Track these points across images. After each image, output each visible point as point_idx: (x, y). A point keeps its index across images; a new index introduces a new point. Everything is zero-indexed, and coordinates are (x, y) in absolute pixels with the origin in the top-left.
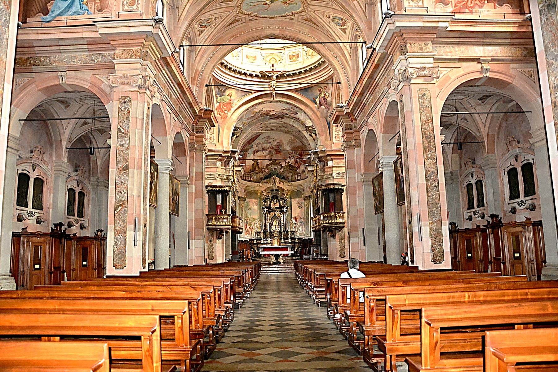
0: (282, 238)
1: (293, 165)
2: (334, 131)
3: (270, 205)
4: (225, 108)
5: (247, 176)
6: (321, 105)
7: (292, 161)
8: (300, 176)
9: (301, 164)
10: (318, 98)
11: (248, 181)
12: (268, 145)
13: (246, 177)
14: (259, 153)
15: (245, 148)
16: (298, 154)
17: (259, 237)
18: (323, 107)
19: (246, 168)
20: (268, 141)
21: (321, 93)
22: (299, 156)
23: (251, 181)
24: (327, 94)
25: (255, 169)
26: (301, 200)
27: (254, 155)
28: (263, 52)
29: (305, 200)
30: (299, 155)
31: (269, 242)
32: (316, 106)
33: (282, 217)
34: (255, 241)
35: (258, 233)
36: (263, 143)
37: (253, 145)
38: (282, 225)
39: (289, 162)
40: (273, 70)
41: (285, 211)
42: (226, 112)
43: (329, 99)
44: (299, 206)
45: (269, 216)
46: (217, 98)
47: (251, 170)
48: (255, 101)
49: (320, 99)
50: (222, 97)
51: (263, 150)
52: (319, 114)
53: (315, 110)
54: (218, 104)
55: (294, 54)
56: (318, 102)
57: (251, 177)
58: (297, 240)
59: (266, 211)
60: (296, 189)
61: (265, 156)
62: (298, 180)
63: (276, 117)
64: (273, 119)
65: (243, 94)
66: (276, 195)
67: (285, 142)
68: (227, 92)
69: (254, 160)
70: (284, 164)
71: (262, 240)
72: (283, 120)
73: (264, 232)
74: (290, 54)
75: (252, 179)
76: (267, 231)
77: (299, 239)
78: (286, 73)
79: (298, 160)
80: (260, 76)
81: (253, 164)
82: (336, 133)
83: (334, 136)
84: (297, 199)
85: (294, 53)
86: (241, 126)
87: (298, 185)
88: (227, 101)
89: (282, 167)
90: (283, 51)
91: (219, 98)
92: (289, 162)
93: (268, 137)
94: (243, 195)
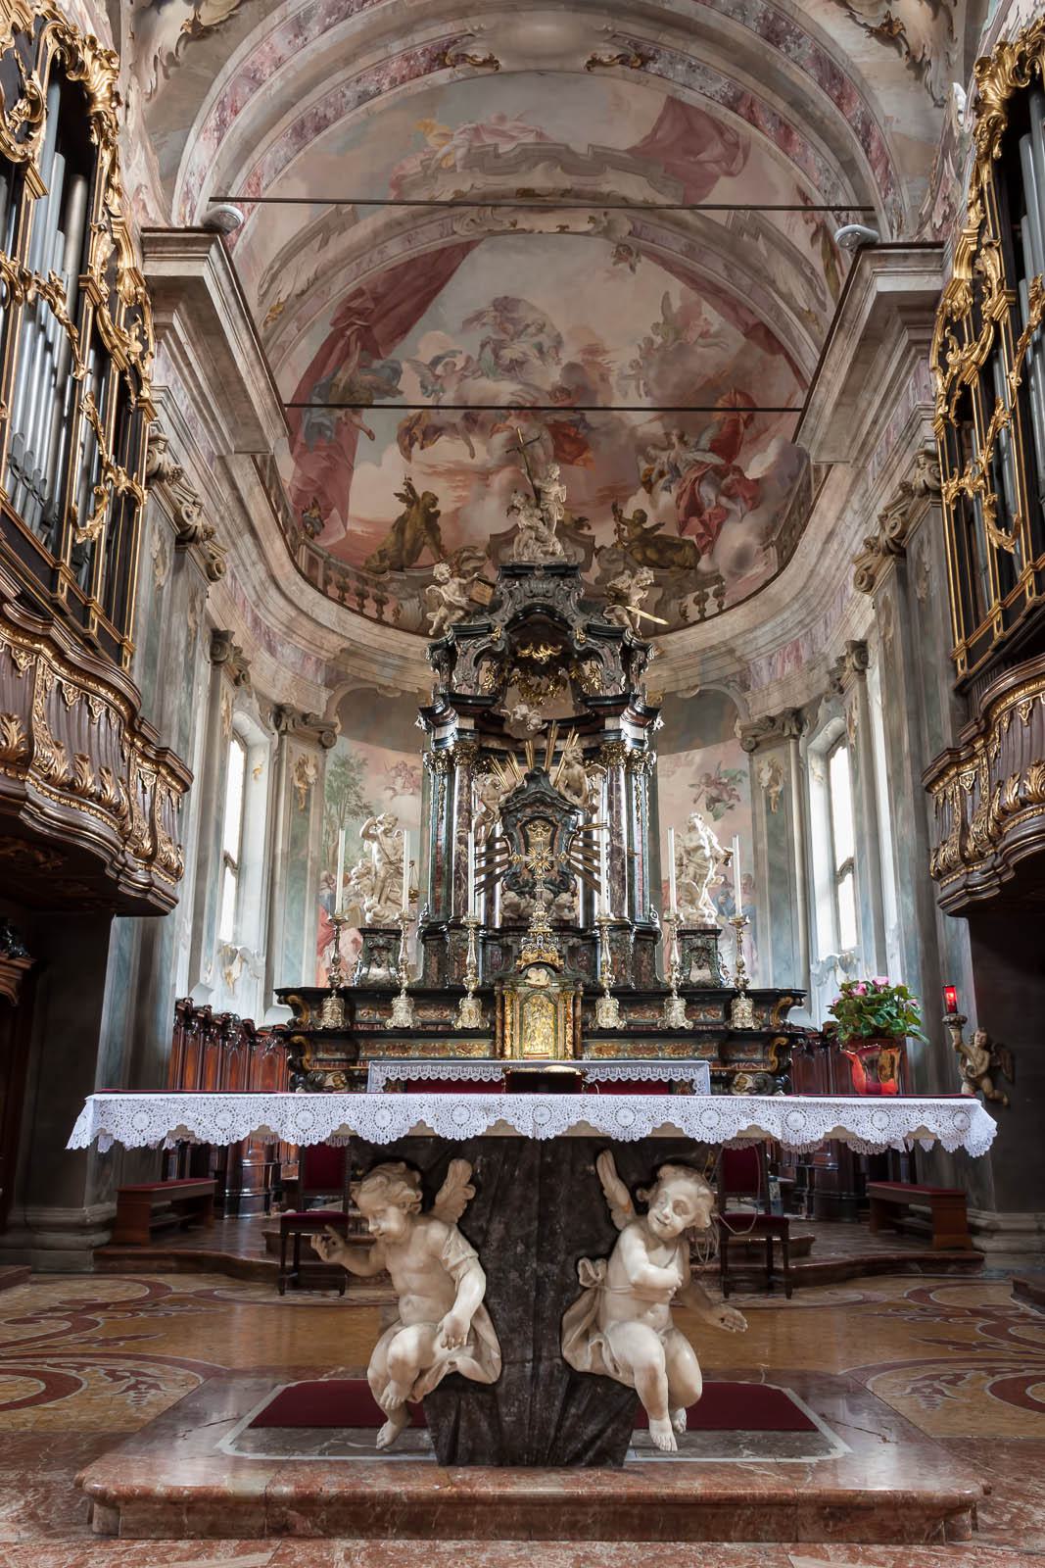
0: (606, 979)
1: (670, 531)
3: (497, 695)
5: (353, 584)
7: (659, 507)
8: (718, 594)
9: (728, 512)
11: (361, 614)
12: (505, 390)
13: (343, 588)
14: (448, 450)
15: (343, 377)
16: (705, 442)
17: (378, 973)
19: (350, 534)
20: (508, 354)
22: (714, 459)
23: (379, 621)
25: (414, 554)
26: (728, 755)
27: (407, 452)
29: (754, 748)
30: (712, 450)
31: (469, 1013)
33: (601, 801)
34: (331, 1005)
35: (379, 939)
36: (472, 369)
37: (397, 373)
38: (604, 864)
39: (642, 517)
41: (629, 746)
44: (712, 802)
45: (482, 784)
47: (382, 555)
51: (474, 417)
57: (381, 602)
58: (744, 1008)
59: (450, 743)
60: (688, 683)
61: (484, 475)
62: (704, 619)
66: (550, 611)
67: (621, 357)
69: (409, 496)
70: (604, 534)
71: (401, 1003)
73: (431, 934)
75: (388, 616)
76: (458, 926)
77: (765, 999)
79: (707, 493)
81: (400, 525)
84: (697, 755)
87: (707, 654)
89: (592, 550)
92: (642, 517)
93: (505, 306)
94: (318, 702)
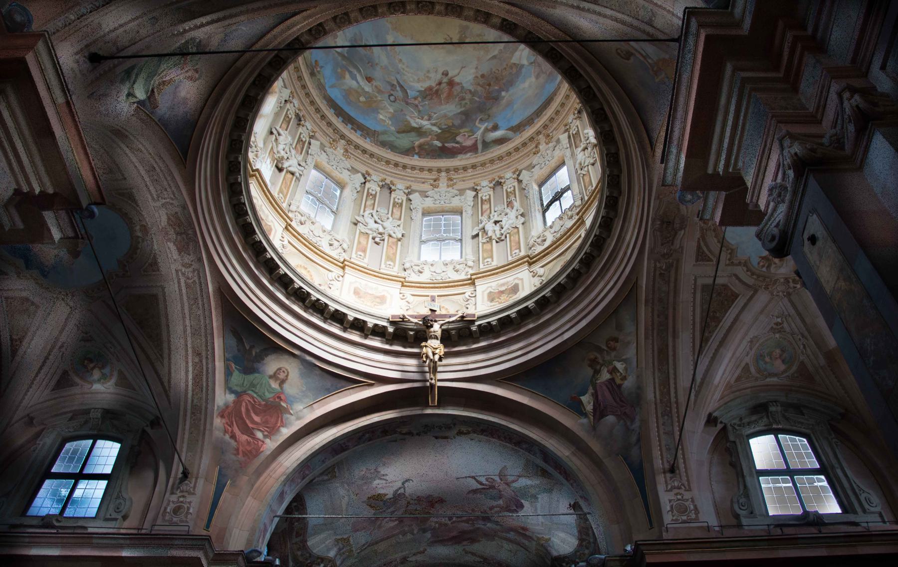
2: (661, 488)
4: (257, 419)
6: (600, 412)
10: (591, 390)
18: (611, 419)
21: (597, 372)
24: (620, 366)
28: (408, 292)
32: (584, 421)
40: (433, 311)
42: (259, 435)
43: (629, 384)
46: (228, 373)
48: (368, 417)
49: (595, 396)
50: (251, 377)
52: (595, 446)
53: (582, 434)
54: (231, 398)
55: (503, 288)
56: (589, 408)
63: (454, 538)
64: (442, 542)
65: (329, 382)
68: (272, 364)
72: (476, 547)
74: (490, 290)
78: (477, 323)
80: (391, 330)
82: (672, 495)
83: (666, 506)
85: (503, 285)
86: (332, 554)
88: (268, 395)
90: (468, 290)
91: (237, 377)
